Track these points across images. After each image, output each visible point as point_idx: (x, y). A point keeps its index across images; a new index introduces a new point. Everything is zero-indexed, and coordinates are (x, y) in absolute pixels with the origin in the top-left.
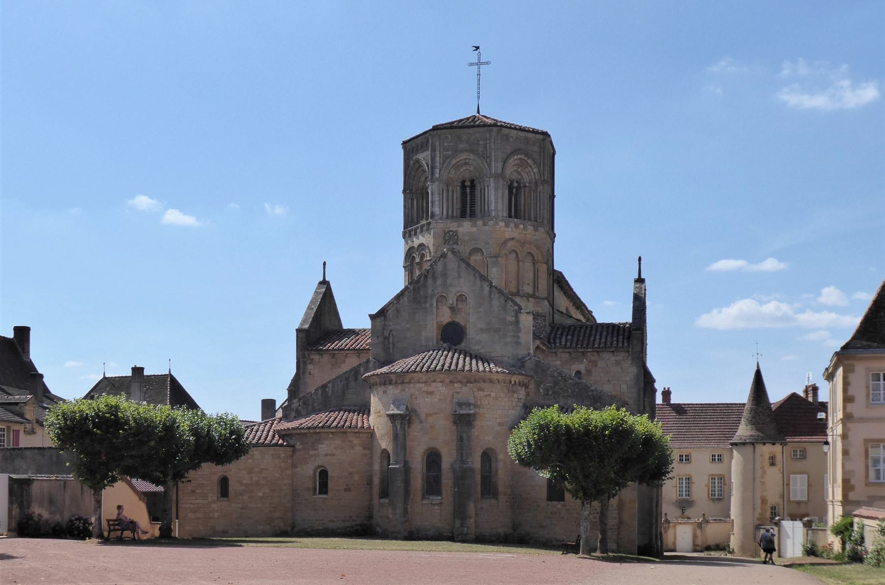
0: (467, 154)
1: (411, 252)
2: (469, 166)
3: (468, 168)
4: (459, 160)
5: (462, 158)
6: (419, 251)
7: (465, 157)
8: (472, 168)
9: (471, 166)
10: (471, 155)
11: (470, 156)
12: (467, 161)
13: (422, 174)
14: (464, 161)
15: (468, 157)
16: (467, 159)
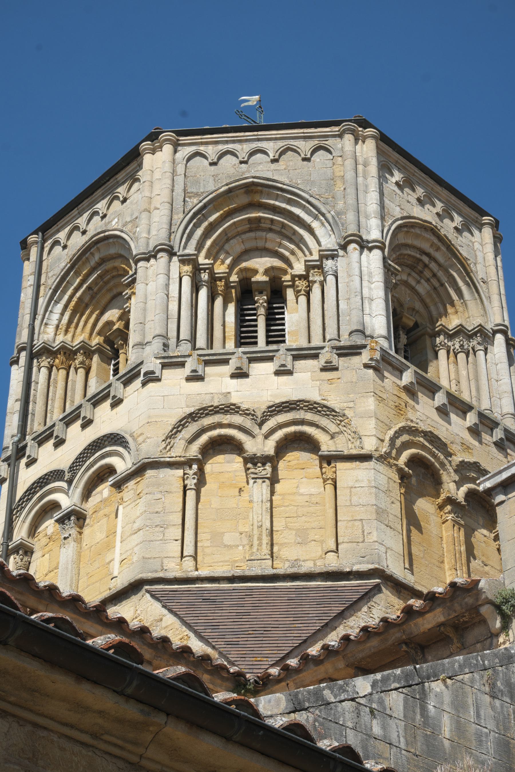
0: (436, 241)
1: (207, 421)
2: (416, 275)
3: (413, 283)
4: (409, 241)
5: (417, 243)
6: (271, 423)
7: (426, 246)
8: (423, 288)
9: (423, 281)
10: (443, 248)
11: (438, 249)
12: (426, 259)
13: (239, 234)
14: (418, 256)
15: (431, 251)
16: (428, 255)
